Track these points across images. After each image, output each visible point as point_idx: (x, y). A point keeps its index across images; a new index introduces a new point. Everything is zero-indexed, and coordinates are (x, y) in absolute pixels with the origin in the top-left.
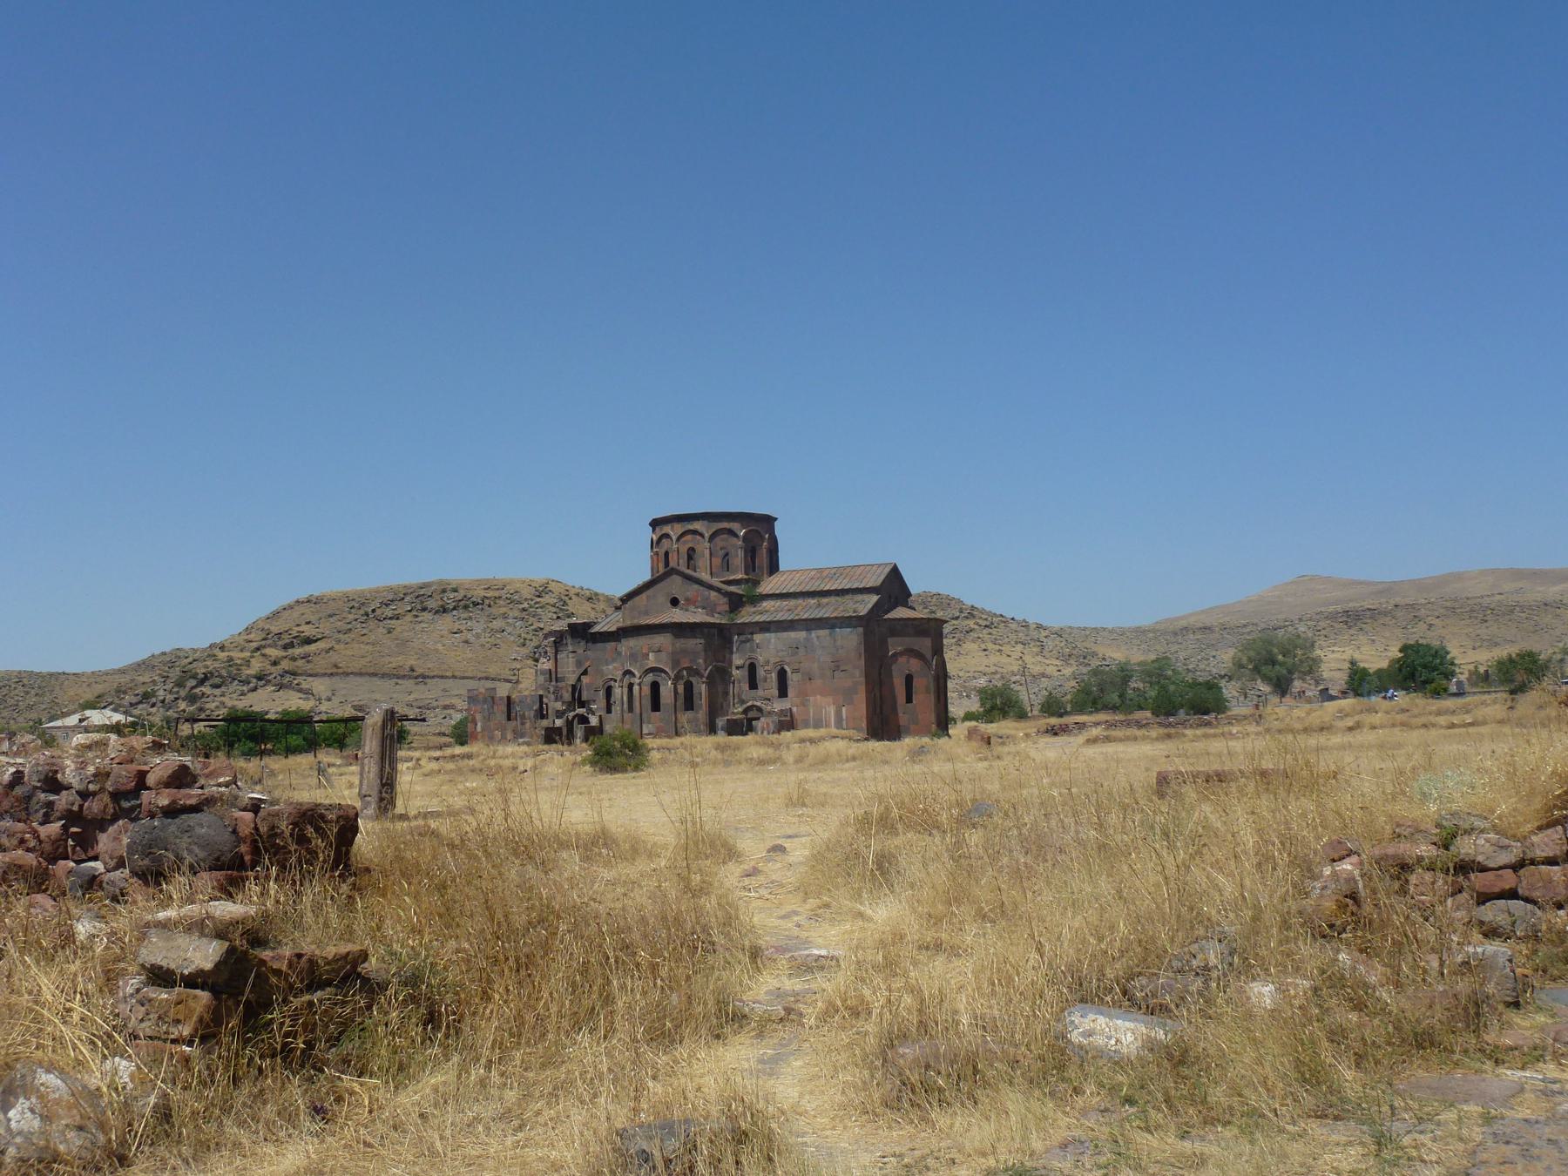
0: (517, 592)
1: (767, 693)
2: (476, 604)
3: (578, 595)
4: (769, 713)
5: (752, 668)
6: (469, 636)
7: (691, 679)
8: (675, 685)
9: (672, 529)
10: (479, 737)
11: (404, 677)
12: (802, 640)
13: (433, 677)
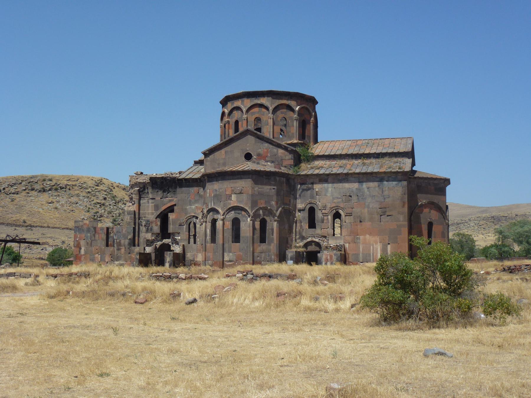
0: (85, 183)
1: (324, 232)
2: (62, 188)
3: (118, 186)
4: (327, 247)
5: (312, 211)
6: (58, 205)
7: (265, 217)
8: (254, 222)
9: (242, 103)
10: (82, 259)
11: (19, 226)
12: (354, 189)
13: (36, 227)
